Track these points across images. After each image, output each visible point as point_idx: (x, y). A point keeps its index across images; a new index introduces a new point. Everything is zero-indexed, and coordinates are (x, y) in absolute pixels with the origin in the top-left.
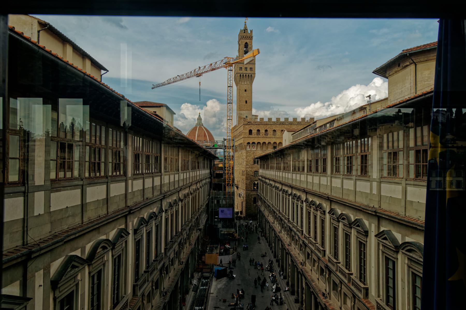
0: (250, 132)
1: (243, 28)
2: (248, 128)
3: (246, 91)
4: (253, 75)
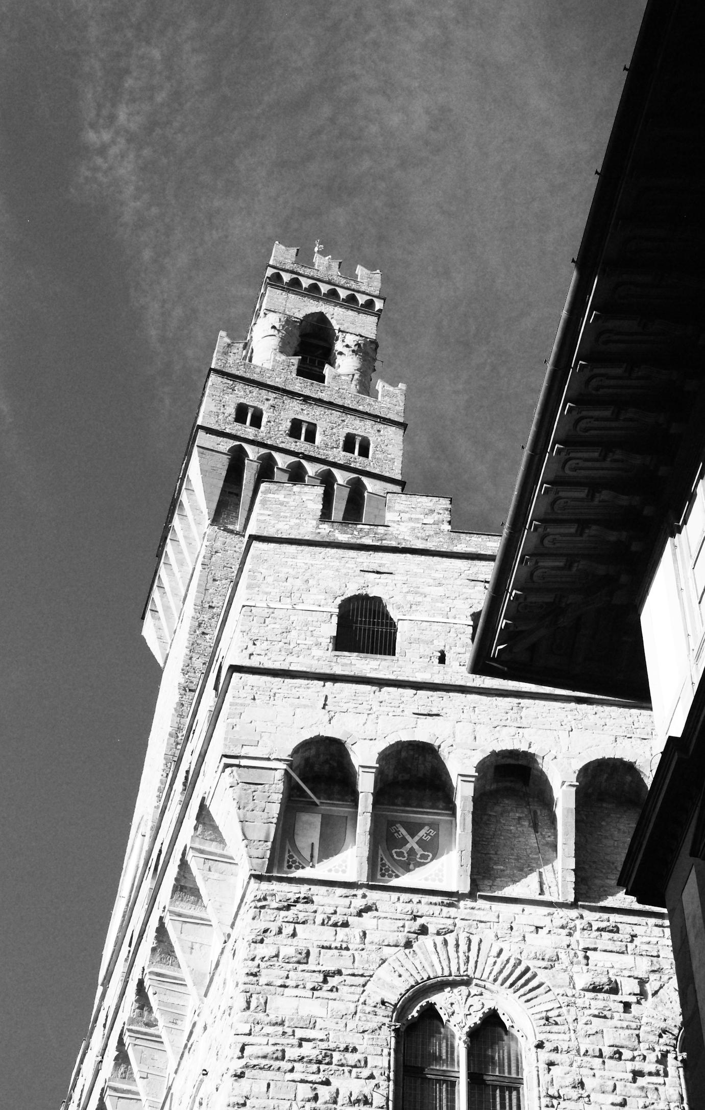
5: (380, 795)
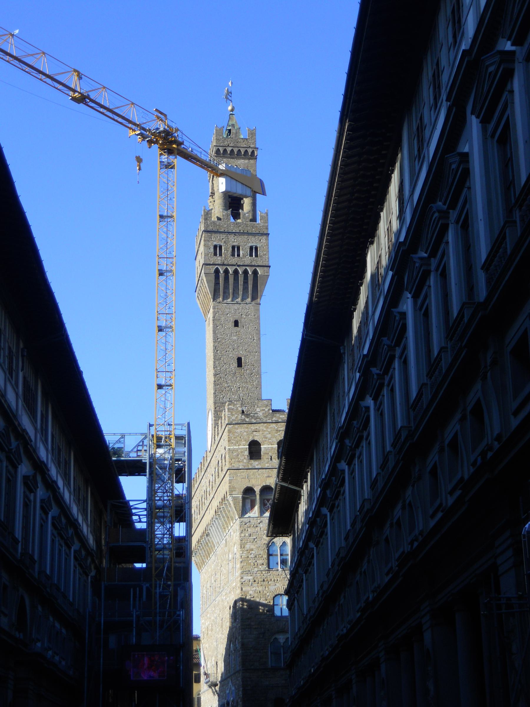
0: (254, 450)
1: (223, 122)
2: (246, 434)
3: (236, 324)
4: (260, 271)
5: (260, 495)
